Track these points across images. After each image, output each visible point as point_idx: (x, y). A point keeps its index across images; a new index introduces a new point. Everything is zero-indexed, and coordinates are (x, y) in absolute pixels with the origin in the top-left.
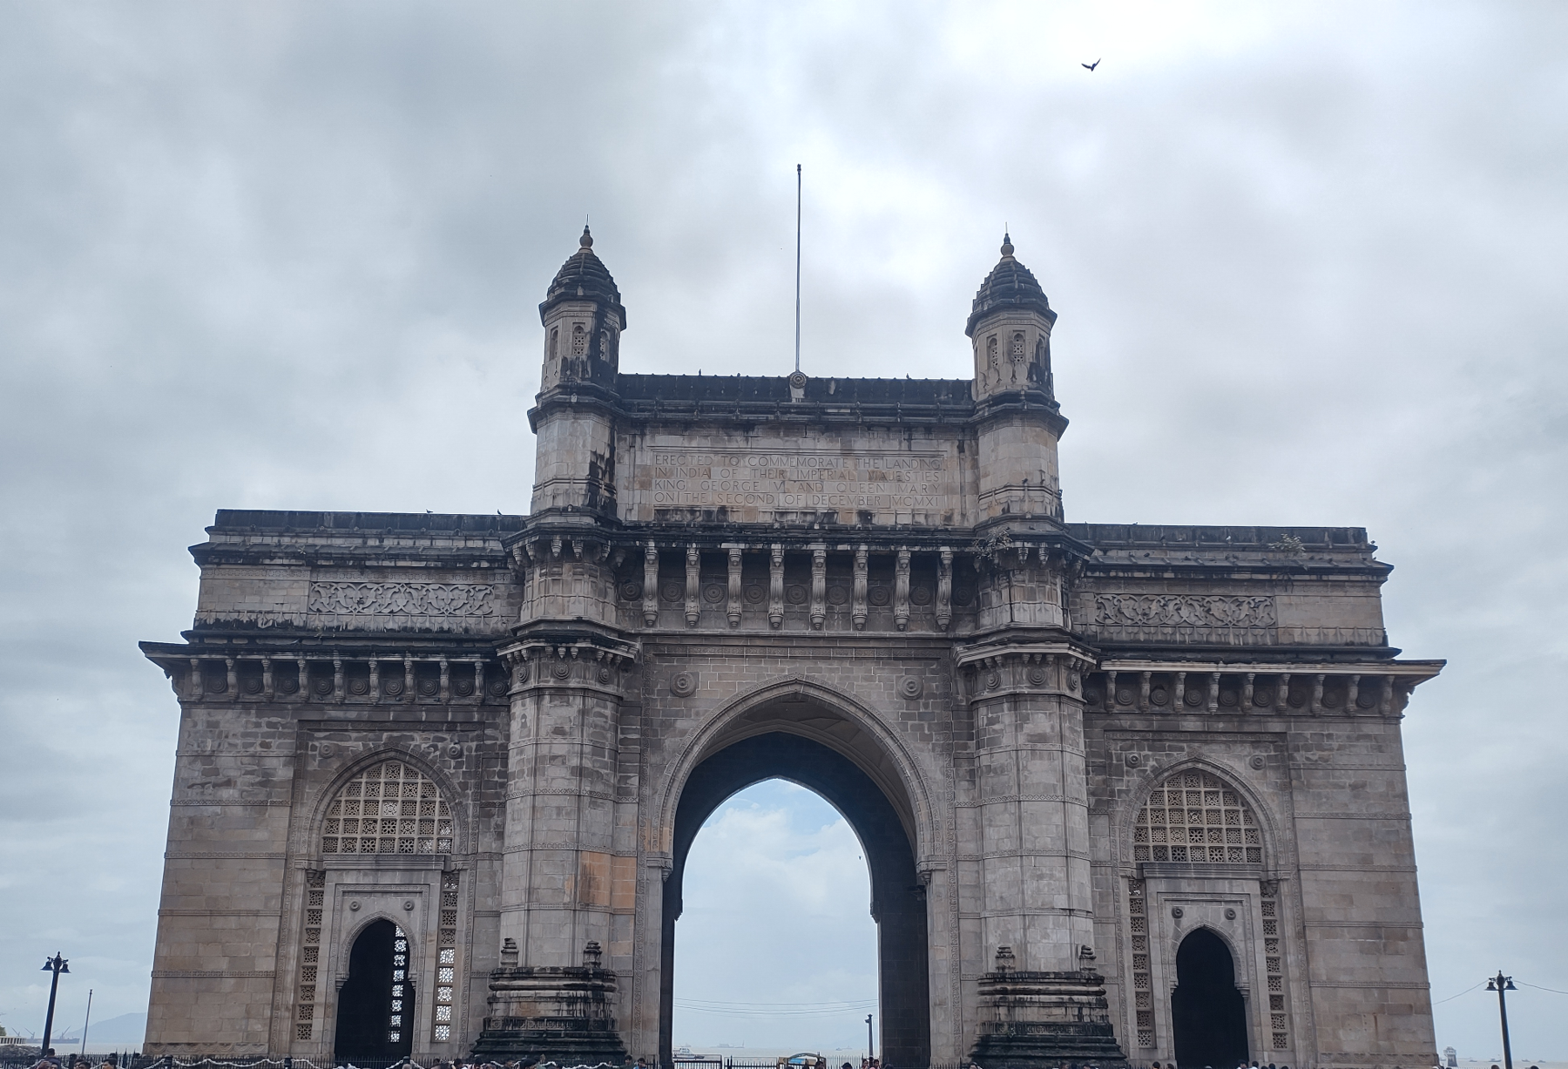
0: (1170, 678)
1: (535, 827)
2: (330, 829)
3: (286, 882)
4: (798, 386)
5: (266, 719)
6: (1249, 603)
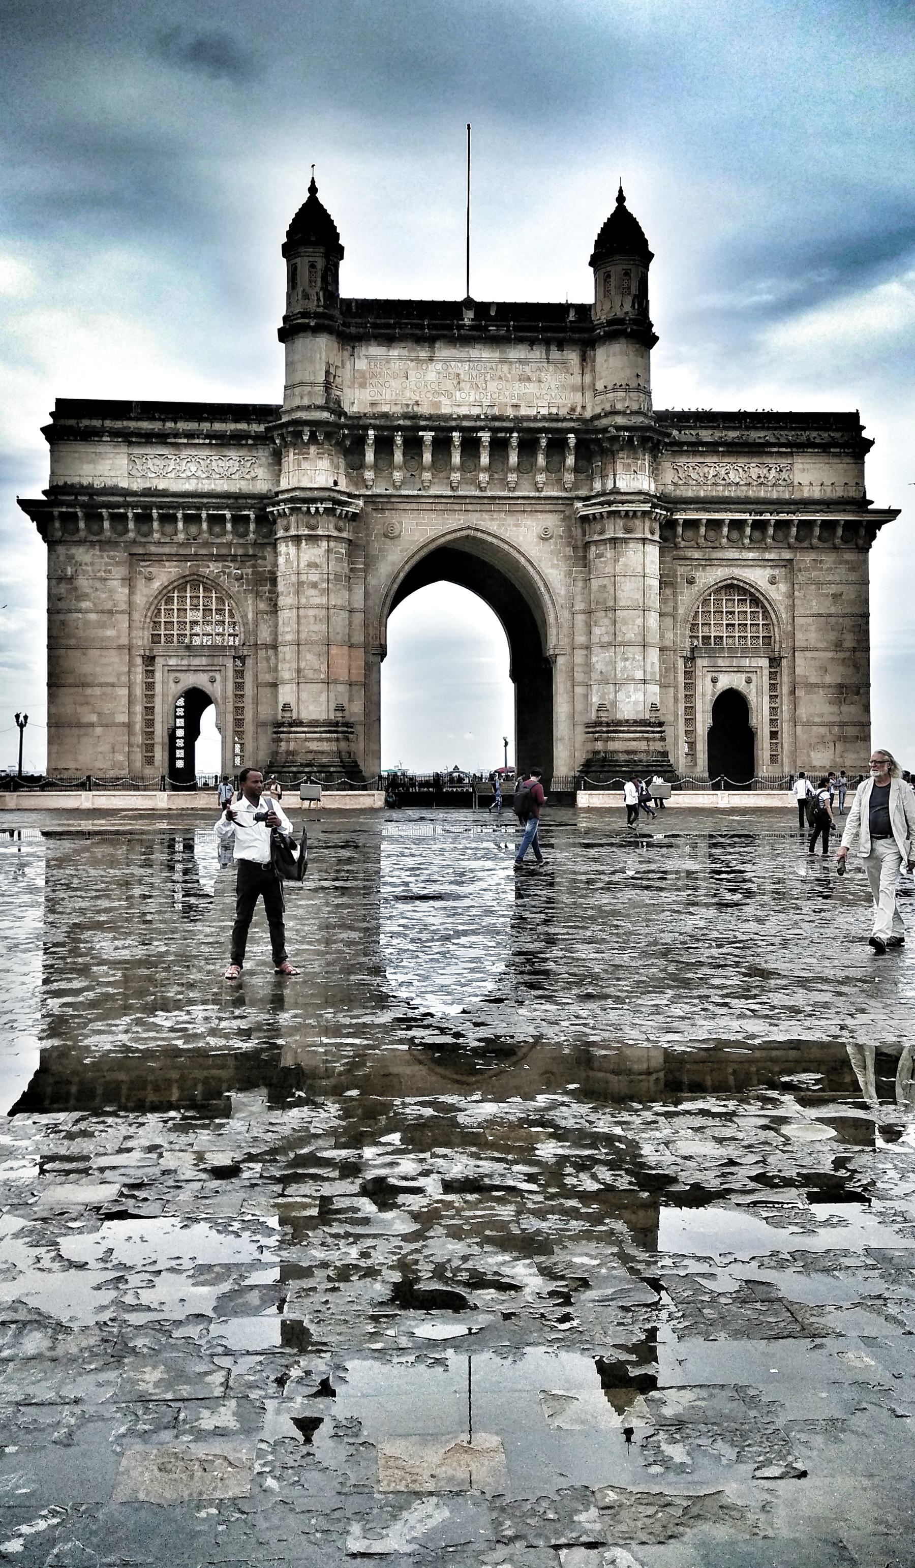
0: (718, 524)
2: (156, 624)
3: (131, 664)
4: (468, 308)
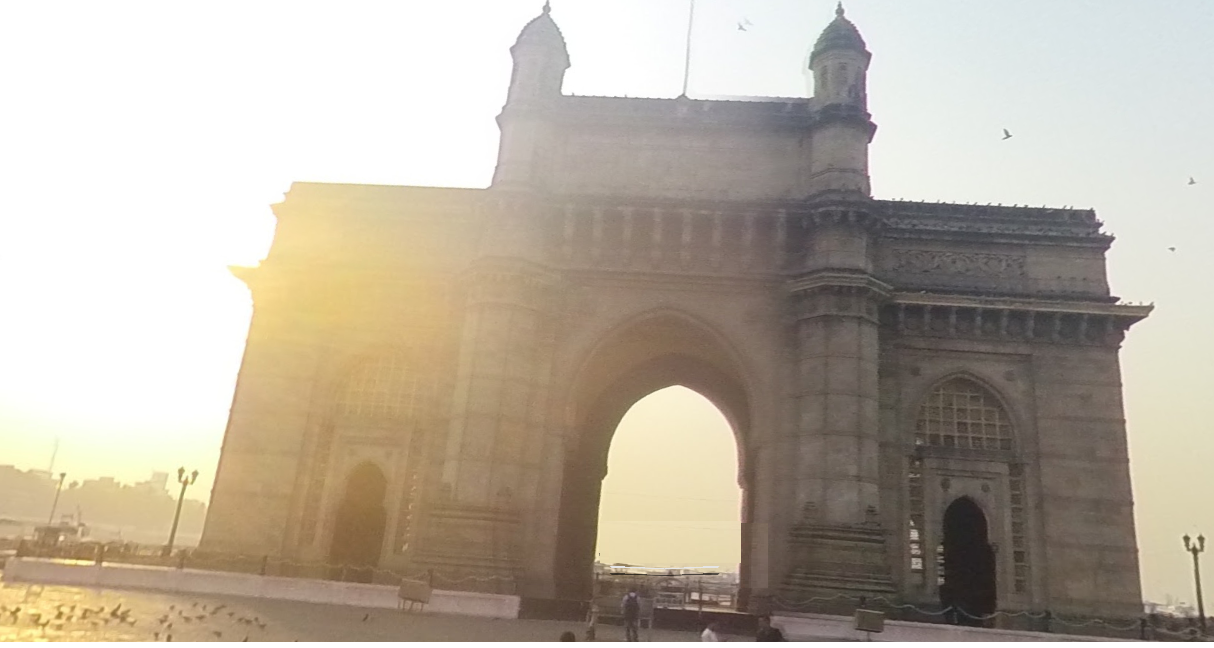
6: (1007, 260)
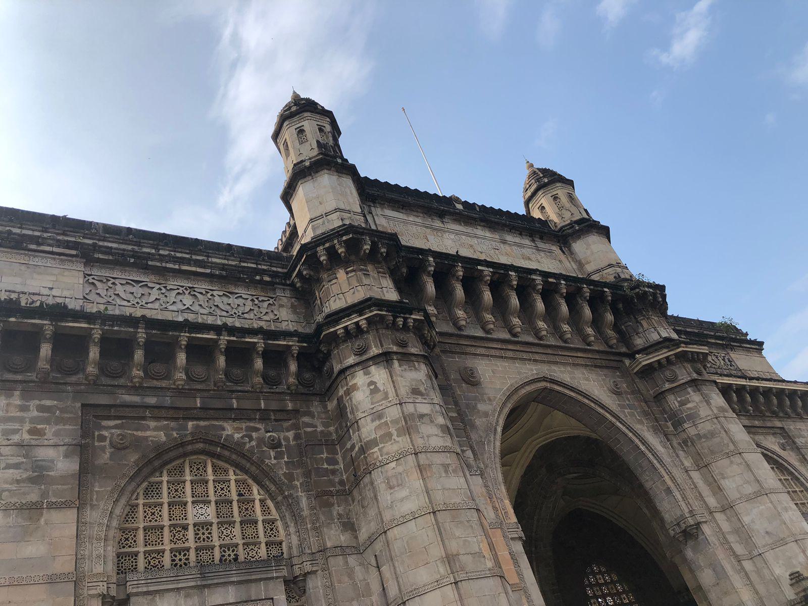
1: (429, 486)
5: (37, 402)
